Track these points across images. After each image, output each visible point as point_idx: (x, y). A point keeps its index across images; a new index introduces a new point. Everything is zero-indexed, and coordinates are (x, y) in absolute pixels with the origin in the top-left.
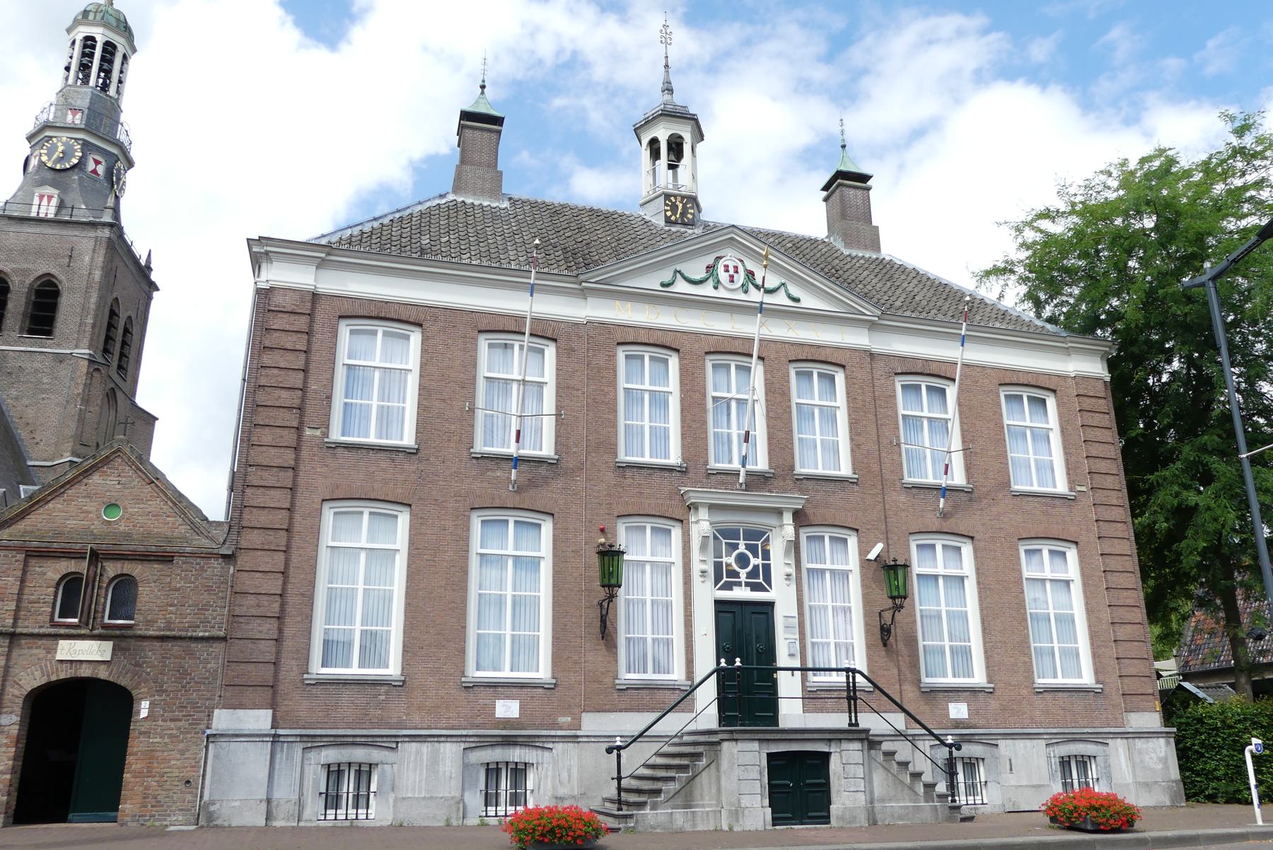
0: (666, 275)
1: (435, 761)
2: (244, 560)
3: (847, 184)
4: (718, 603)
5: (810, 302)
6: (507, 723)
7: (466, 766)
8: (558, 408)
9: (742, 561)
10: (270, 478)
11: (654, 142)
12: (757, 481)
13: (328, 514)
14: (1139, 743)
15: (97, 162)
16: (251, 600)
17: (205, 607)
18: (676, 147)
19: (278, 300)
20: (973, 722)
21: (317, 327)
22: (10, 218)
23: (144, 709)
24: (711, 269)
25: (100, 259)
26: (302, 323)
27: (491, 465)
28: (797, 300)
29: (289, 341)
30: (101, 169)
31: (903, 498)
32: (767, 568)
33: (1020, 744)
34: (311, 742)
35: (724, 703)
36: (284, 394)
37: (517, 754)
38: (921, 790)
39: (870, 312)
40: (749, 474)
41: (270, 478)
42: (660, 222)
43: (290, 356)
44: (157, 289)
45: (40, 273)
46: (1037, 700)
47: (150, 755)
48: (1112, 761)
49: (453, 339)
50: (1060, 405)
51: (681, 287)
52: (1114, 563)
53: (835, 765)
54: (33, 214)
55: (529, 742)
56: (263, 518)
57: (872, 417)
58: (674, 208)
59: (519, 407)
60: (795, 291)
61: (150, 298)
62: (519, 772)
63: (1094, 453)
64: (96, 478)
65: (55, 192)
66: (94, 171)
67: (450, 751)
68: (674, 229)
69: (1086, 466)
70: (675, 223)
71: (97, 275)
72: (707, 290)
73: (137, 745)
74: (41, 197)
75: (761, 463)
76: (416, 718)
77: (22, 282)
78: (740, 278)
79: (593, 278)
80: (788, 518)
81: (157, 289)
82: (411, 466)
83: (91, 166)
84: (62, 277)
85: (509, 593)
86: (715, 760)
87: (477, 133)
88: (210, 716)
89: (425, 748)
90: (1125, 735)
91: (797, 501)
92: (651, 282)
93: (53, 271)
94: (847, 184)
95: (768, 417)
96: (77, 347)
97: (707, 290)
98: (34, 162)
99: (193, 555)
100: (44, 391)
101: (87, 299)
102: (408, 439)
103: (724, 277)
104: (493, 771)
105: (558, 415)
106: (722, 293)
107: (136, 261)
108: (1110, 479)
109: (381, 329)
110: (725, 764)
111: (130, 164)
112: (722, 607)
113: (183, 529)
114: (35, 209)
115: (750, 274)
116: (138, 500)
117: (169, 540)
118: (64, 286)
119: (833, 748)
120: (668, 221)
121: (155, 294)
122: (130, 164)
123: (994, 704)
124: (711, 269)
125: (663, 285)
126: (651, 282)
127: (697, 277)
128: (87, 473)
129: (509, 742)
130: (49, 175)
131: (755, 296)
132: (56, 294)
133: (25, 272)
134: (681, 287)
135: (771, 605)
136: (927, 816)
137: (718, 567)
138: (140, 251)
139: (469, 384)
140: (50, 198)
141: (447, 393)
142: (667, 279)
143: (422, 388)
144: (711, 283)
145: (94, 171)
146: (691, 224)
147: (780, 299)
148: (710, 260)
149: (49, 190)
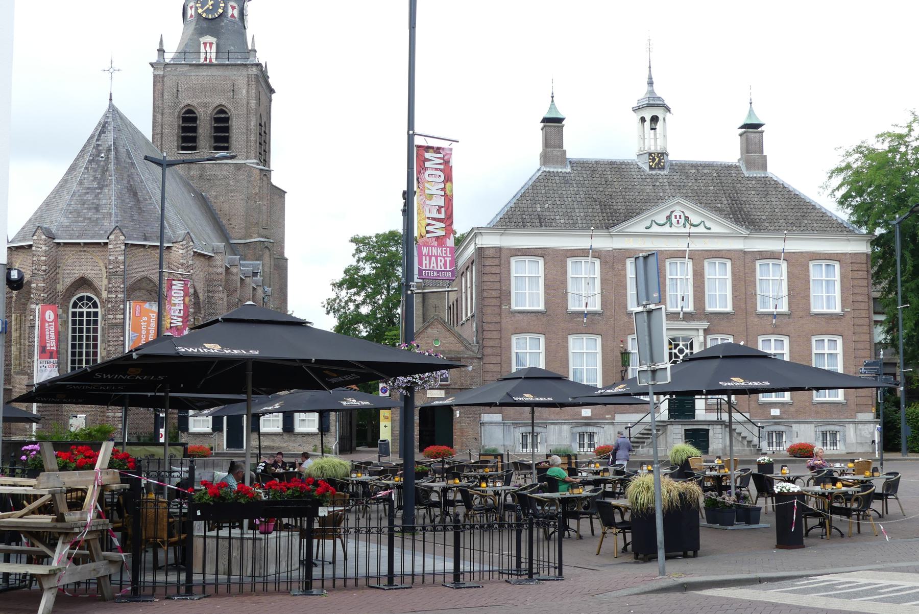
0: (648, 223)
1: (560, 431)
2: (486, 360)
3: (752, 128)
5: (716, 229)
6: (586, 418)
7: (573, 434)
8: (602, 289)
9: (681, 351)
10: (492, 327)
11: (643, 120)
12: (688, 317)
13: (514, 339)
14: (860, 426)
15: (233, 8)
16: (490, 375)
17: (474, 377)
18: (655, 119)
19: (487, 253)
20: (783, 416)
21: (502, 262)
22: (191, 65)
23: (458, 414)
24: (669, 218)
25: (253, 92)
26: (497, 261)
27: (575, 316)
28: (709, 229)
29: (493, 270)
30: (236, 13)
31: (756, 319)
33: (802, 426)
34: (516, 425)
35: (670, 410)
36: (493, 292)
37: (590, 429)
38: (746, 443)
39: (745, 232)
40: (685, 313)
41: (492, 327)
42: (647, 169)
43: (494, 276)
45: (216, 105)
46: (813, 408)
47: (462, 430)
48: (847, 433)
49: (555, 261)
50: (842, 268)
51: (655, 229)
52: (859, 346)
53: (711, 433)
54: (202, 61)
55: (595, 425)
56: (491, 343)
57: (743, 283)
58: (654, 160)
59: (585, 290)
60: (708, 224)
61: (270, 101)
62: (591, 436)
63: (856, 292)
64: (429, 330)
65: (213, 40)
66: (233, 16)
67: (566, 428)
68: (654, 172)
69: (851, 298)
70: (655, 168)
71: (253, 103)
72: (667, 229)
73: (456, 427)
74: (205, 44)
75: (690, 308)
76: (552, 416)
77: (205, 113)
78: (682, 221)
79: (614, 230)
80: (701, 333)
82: (544, 319)
84: (230, 107)
85: (585, 368)
86: (665, 432)
87: (552, 129)
88: (480, 416)
89: (557, 427)
90: (854, 423)
91: (705, 325)
93: (224, 103)
95: (694, 287)
96: (247, 158)
97: (667, 229)
98: (191, 12)
99: (467, 358)
100: (231, 191)
101: (248, 122)
102: (541, 307)
103: (674, 221)
104: (581, 436)
105: (602, 293)
106: (673, 230)
108: (863, 304)
109: (527, 259)
110: (669, 433)
113: (462, 348)
114: (202, 56)
115: (687, 218)
116: (445, 338)
117: (458, 352)
118: (232, 111)
119: (710, 427)
120: (651, 168)
121: (273, 96)
123: (792, 409)
124: (669, 218)
126: (640, 228)
127: (662, 222)
128: (426, 329)
129: (587, 425)
130: (205, 24)
132: (227, 120)
133: (206, 105)
134: (655, 229)
136: (748, 452)
137: (670, 354)
139: (564, 282)
140: (211, 44)
141: (556, 286)
142: (648, 225)
143: (545, 285)
144: (668, 224)
145: (233, 16)
146: (663, 168)
147: (701, 229)
148: (668, 213)
149: (209, 39)
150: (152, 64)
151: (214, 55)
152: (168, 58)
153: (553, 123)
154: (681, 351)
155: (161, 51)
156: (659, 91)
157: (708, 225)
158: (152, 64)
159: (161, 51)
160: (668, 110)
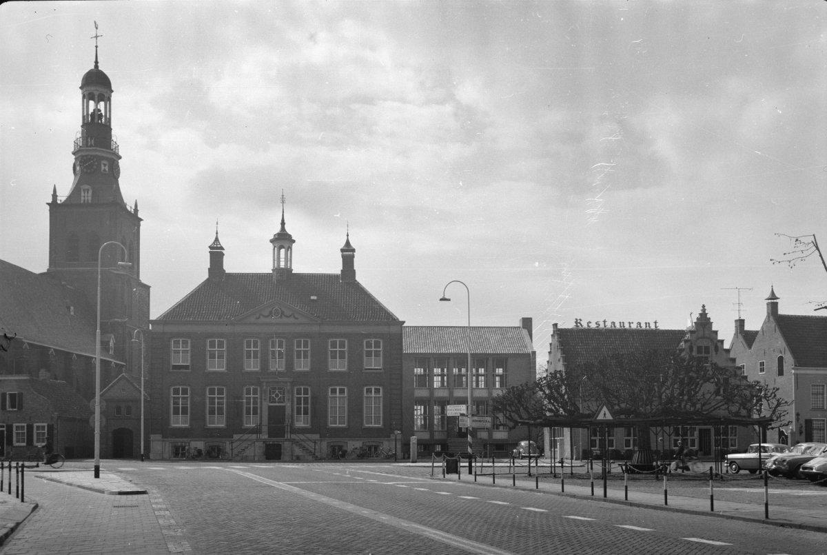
0: (258, 316)
3: (348, 254)
4: (270, 407)
9: (277, 395)
15: (105, 165)
32: (284, 397)
44: (142, 220)
51: (262, 320)
66: (105, 170)
72: (267, 320)
74: (84, 190)
81: (142, 220)
83: (103, 168)
92: (253, 319)
94: (348, 254)
107: (130, 212)
111: (120, 158)
112: (270, 407)
114: (82, 198)
122: (120, 158)
124: (271, 312)
125: (257, 318)
131: (285, 320)
134: (262, 320)
135: (284, 406)
137: (270, 397)
138: (130, 206)
140: (88, 190)
148: (270, 309)
149: (87, 187)
150: (48, 204)
151: (90, 198)
152: (62, 198)
153: (216, 254)
154: (277, 395)
155: (55, 196)
156: (288, 229)
157: (296, 316)
158: (48, 204)
159: (55, 196)
160: (294, 241)
